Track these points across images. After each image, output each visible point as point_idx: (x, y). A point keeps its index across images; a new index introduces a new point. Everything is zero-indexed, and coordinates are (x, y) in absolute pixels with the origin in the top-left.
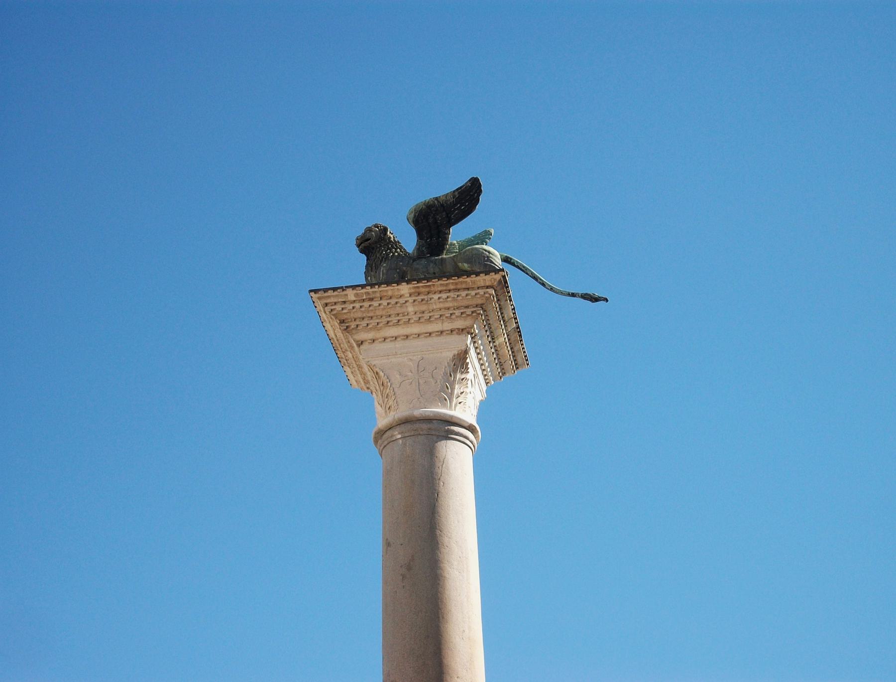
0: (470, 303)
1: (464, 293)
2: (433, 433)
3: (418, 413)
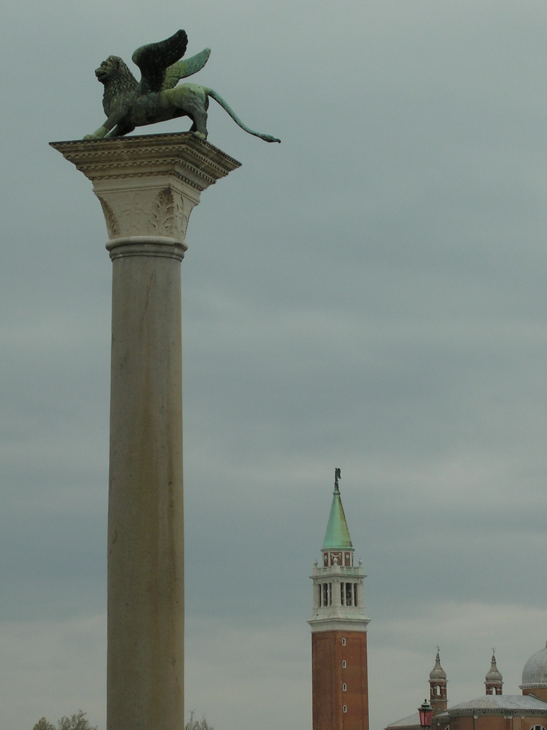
1: (163, 148)
2: (145, 254)
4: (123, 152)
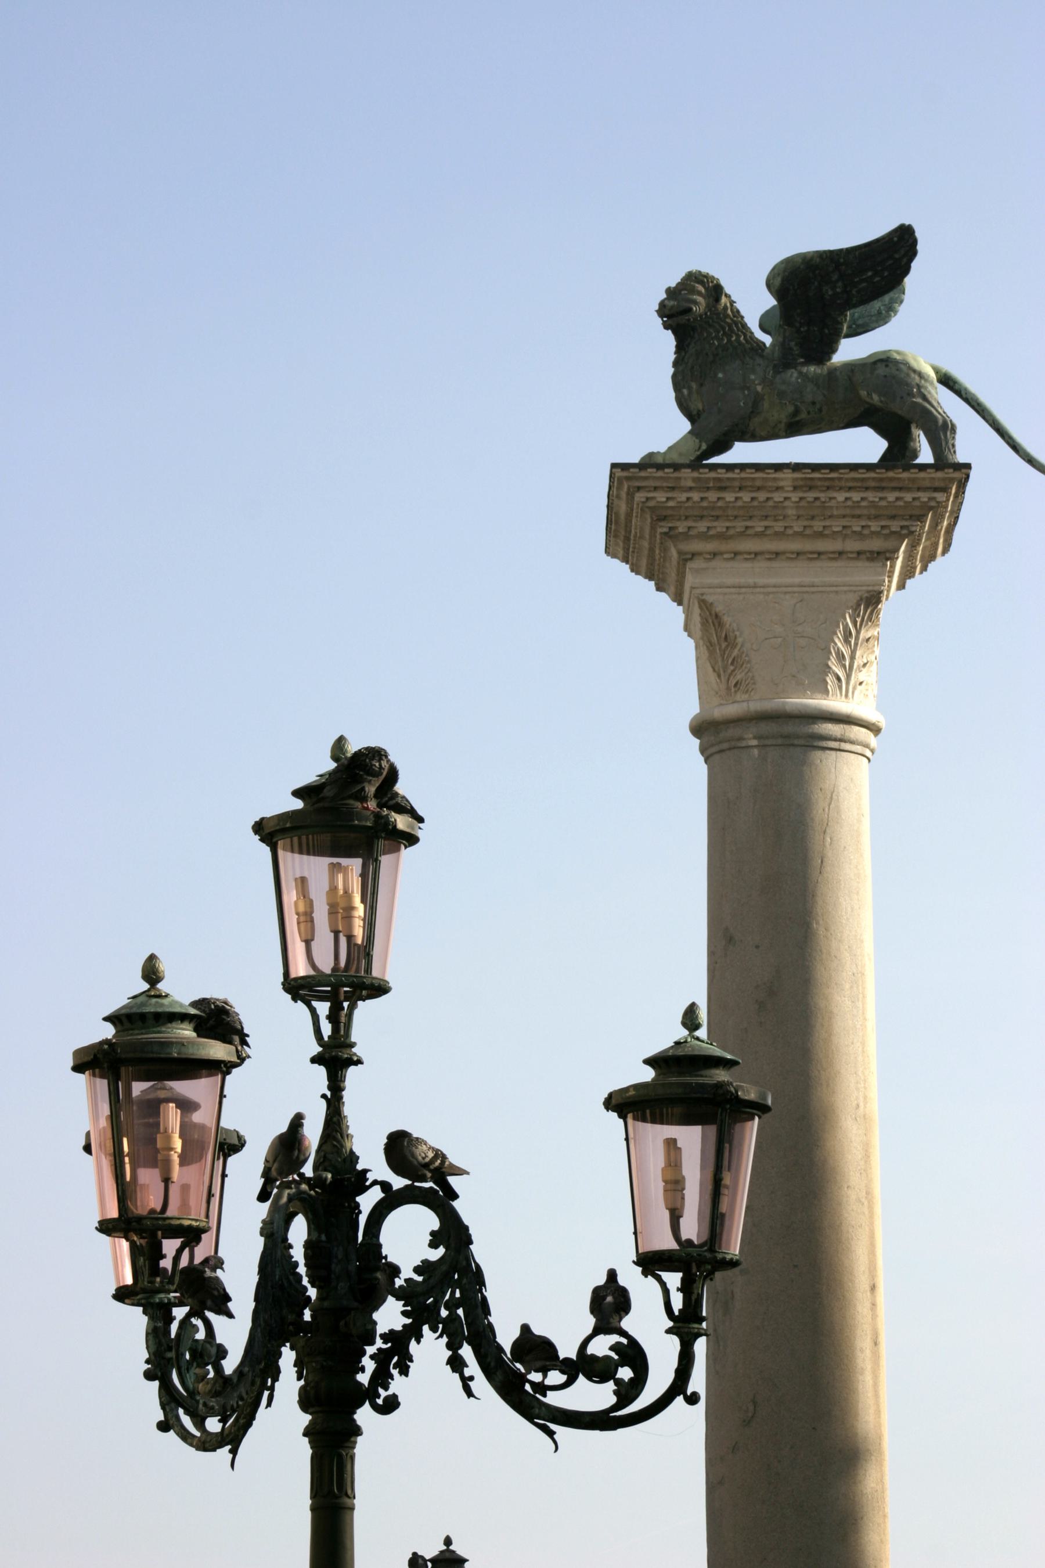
1: (891, 496)
4: (786, 499)
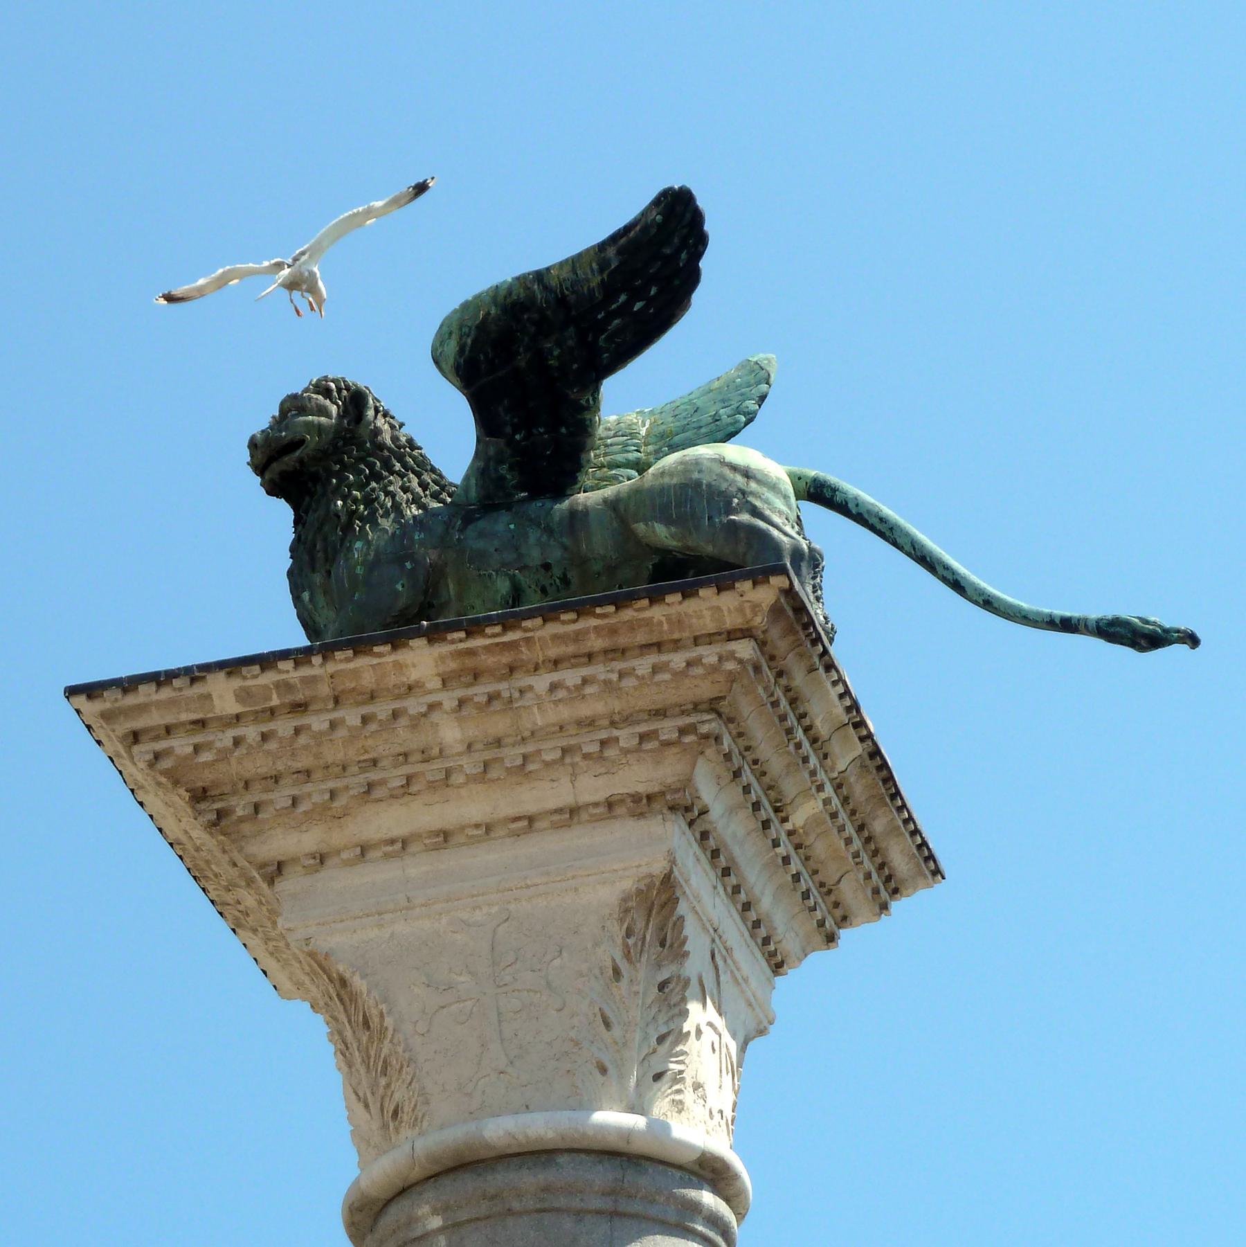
0: (671, 696)
1: (643, 665)
2: (562, 1202)
3: (500, 1130)
4: (432, 707)
